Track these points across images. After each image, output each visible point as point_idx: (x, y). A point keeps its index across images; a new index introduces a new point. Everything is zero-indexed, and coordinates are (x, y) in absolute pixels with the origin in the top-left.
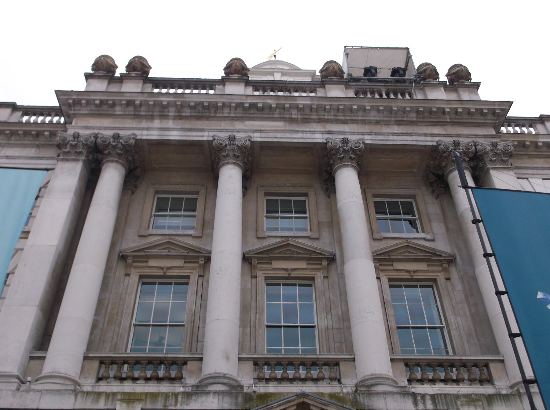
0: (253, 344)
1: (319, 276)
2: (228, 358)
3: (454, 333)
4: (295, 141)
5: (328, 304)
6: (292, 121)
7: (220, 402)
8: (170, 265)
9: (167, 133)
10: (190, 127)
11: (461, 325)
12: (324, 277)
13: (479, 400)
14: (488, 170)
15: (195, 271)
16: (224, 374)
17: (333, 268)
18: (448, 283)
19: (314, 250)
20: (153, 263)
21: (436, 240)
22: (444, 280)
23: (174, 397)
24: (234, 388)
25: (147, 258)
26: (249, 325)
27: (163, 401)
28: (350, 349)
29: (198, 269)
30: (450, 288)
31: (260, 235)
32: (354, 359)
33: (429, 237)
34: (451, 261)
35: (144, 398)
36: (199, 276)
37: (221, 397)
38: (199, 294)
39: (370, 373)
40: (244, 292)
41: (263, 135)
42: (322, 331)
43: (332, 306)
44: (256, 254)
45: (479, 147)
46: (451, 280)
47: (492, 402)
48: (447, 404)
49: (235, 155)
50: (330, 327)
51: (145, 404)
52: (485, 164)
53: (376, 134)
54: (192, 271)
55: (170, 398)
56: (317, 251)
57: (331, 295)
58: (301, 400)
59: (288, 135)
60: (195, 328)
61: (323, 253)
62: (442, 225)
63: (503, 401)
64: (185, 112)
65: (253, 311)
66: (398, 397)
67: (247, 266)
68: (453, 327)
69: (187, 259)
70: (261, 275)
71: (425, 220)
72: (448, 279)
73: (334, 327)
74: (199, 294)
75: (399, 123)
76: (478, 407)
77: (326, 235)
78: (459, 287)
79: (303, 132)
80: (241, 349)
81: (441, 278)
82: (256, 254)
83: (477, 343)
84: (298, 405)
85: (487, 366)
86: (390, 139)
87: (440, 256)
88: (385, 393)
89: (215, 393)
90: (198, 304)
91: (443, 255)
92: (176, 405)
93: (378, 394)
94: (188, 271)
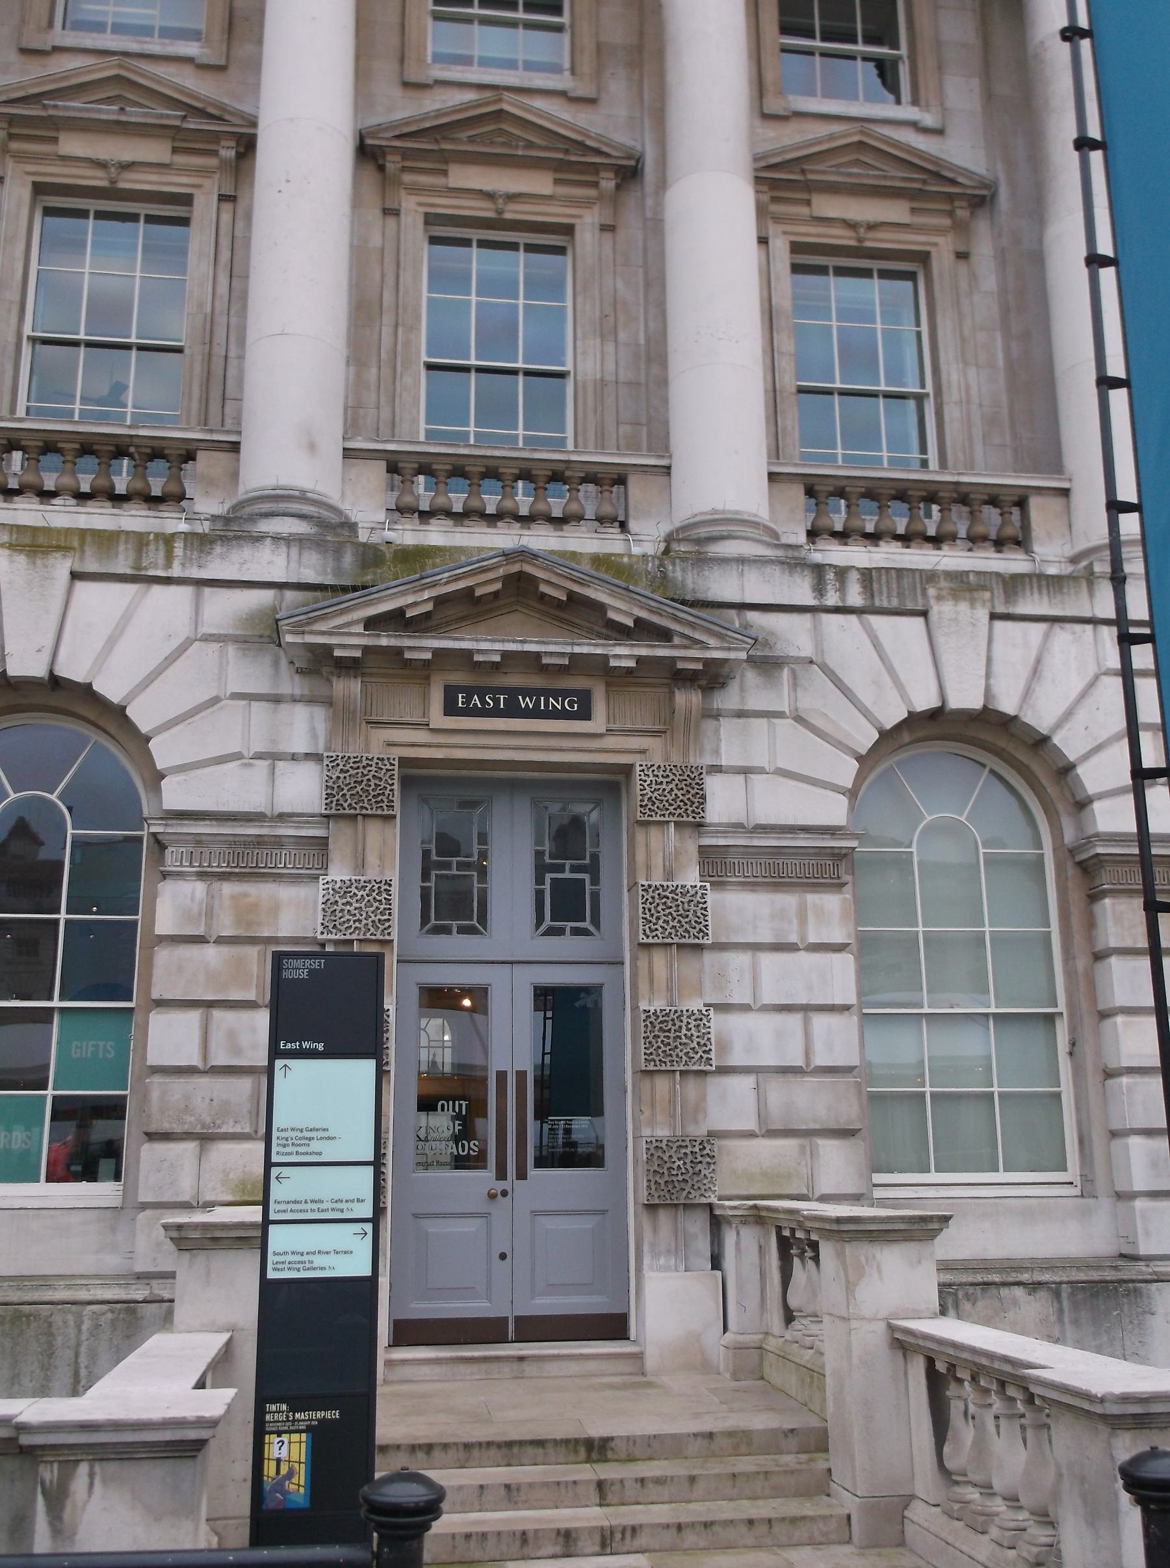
0: (385, 413)
1: (587, 222)
2: (312, 447)
3: (952, 413)
5: (608, 310)
7: (293, 565)
8: (127, 156)
11: (974, 392)
13: (984, 588)
15: (207, 183)
16: (304, 492)
17: (630, 199)
18: (962, 268)
20: (72, 145)
21: (949, 130)
22: (952, 257)
23: (162, 547)
24: (332, 530)
25: (56, 126)
26: (374, 359)
27: (132, 555)
28: (661, 441)
29: (217, 176)
30: (964, 285)
31: (413, 76)
34: (981, 200)
35: (76, 544)
36: (222, 198)
37: (294, 551)
38: (225, 255)
39: (707, 508)
40: (359, 256)
43: (622, 318)
46: (974, 259)
47: (1016, 593)
48: (900, 595)
50: (609, 377)
51: (82, 559)
55: (152, 547)
56: (589, 143)
57: (620, 285)
58: (515, 568)
60: (214, 359)
62: (976, 82)
63: (1045, 591)
65: (388, 319)
66: (776, 571)
67: (370, 172)
68: (952, 395)
69: (183, 141)
70: (412, 208)
71: (927, 63)
74: (225, 255)
76: (978, 605)
77: (617, 87)
78: (989, 281)
80: (352, 426)
81: (943, 249)
83: (1008, 442)
84: (508, 579)
85: (1021, 503)
87: (952, 182)
88: (742, 561)
89: (277, 538)
90: (223, 289)
91: (960, 180)
92: (168, 564)
93: (724, 561)
94: (185, 180)
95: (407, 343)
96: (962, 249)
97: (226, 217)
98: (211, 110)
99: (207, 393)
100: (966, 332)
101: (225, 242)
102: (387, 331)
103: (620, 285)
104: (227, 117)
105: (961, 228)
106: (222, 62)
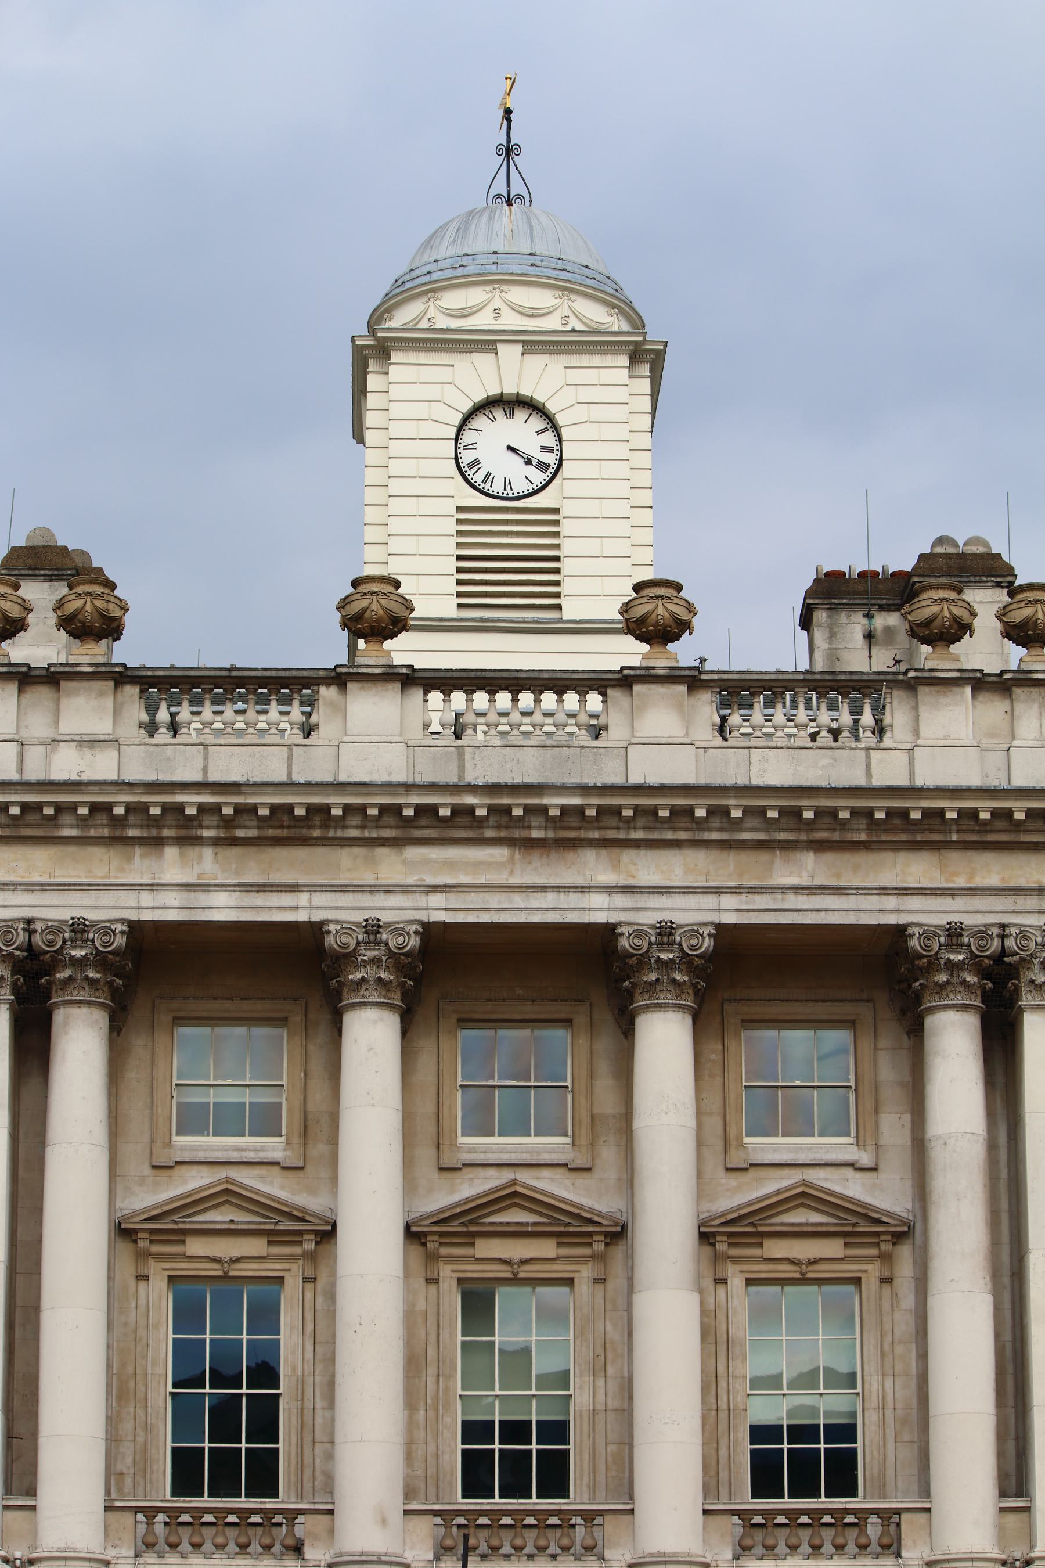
0: (431, 1448)
2: (384, 1521)
4: (536, 918)
5: (600, 1350)
6: (530, 844)
8: (237, 1253)
9: (202, 899)
10: (261, 881)
12: (596, 1281)
14: (1021, 1011)
15: (294, 1267)
16: (379, 1555)
18: (886, 1289)
19: (577, 1211)
20: (196, 1246)
21: (881, 1166)
22: (878, 1282)
25: (182, 1235)
26: (422, 1404)
29: (301, 1262)
30: (886, 1306)
31: (447, 1163)
32: (632, 1511)
33: (865, 1158)
36: (306, 1280)
38: (310, 1327)
39: (654, 1550)
40: (410, 1319)
41: (454, 900)
42: (581, 1417)
43: (610, 1356)
44: (435, 1223)
45: (1011, 943)
46: (896, 1282)
49: (380, 978)
50: (600, 1407)
52: (1016, 993)
53: (753, 890)
54: (286, 1266)
56: (584, 1214)
57: (609, 1327)
59: (518, 900)
60: (306, 1412)
61: (596, 1219)
62: (907, 1117)
64: (245, 827)
65: (432, 1370)
67: (417, 1251)
69: (273, 1237)
70: (447, 1273)
72: (887, 1281)
73: (610, 1406)
74: (310, 1327)
75: (820, 846)
79: (558, 888)
80: (409, 1494)
82: (435, 1223)
83: (916, 1439)
86: (786, 906)
87: (878, 1222)
90: (309, 1355)
91: (885, 1219)
94: (278, 1266)
95: (446, 1390)
96: (886, 1274)
97: (309, 1295)
98: (295, 1213)
99: (302, 1439)
100: (887, 1347)
101: (309, 1316)
102: (431, 1380)
103: (609, 1327)
104: (308, 1218)
105: (885, 1258)
106: (300, 1165)
